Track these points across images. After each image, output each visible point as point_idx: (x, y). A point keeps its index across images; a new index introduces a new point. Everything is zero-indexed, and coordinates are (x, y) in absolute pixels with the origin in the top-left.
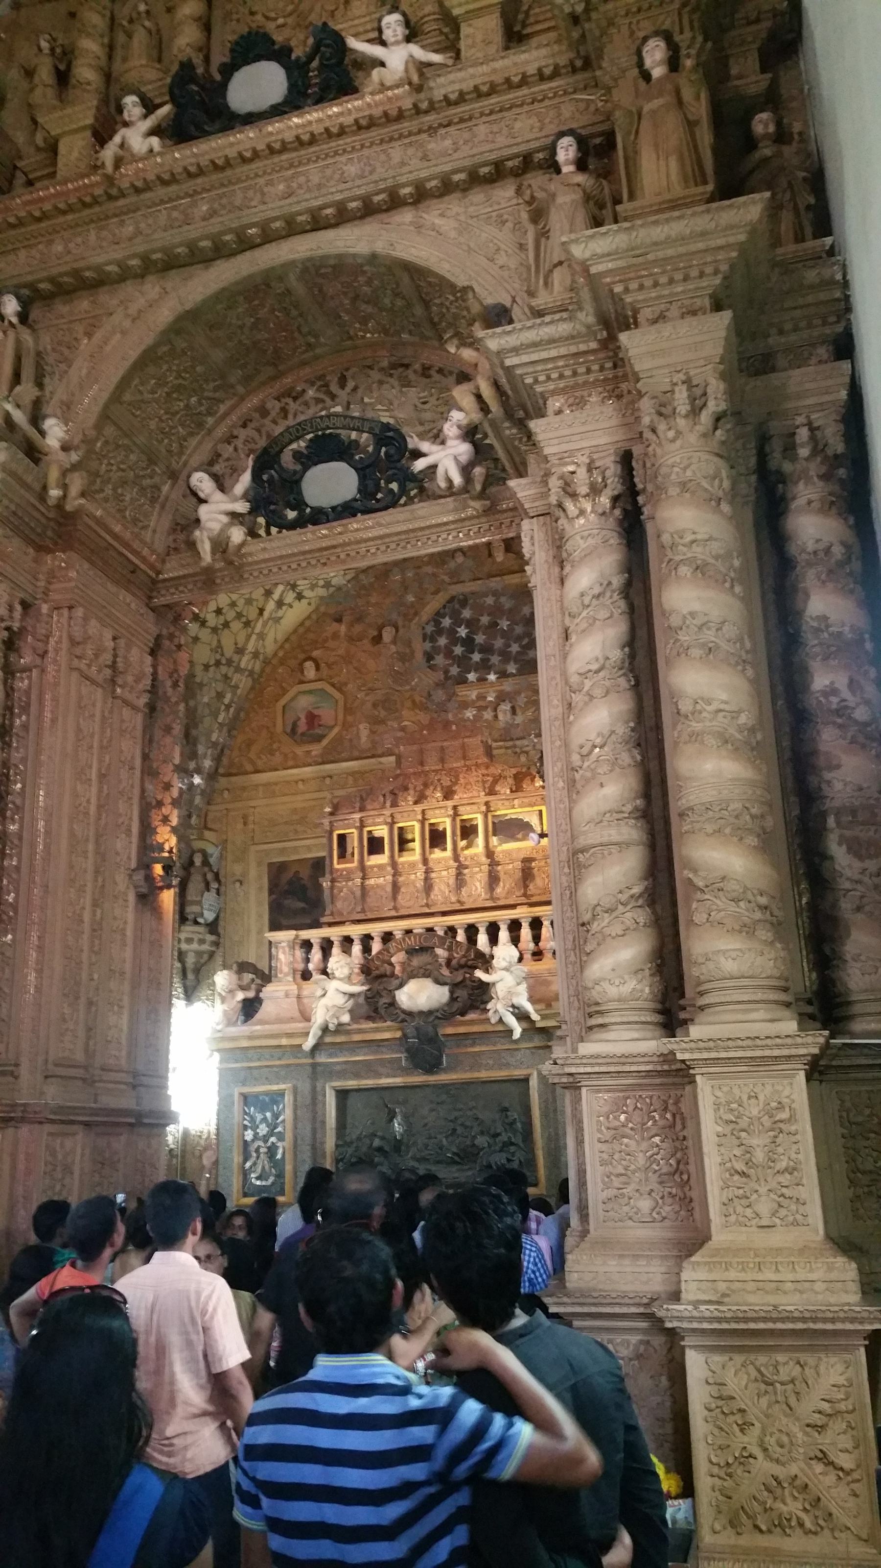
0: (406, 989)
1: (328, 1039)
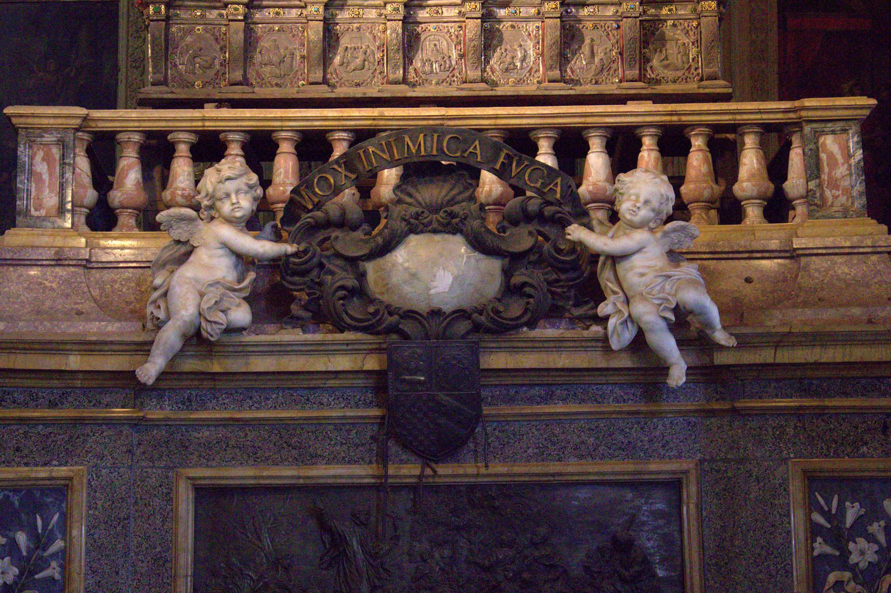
0: (400, 256)
1: (190, 365)
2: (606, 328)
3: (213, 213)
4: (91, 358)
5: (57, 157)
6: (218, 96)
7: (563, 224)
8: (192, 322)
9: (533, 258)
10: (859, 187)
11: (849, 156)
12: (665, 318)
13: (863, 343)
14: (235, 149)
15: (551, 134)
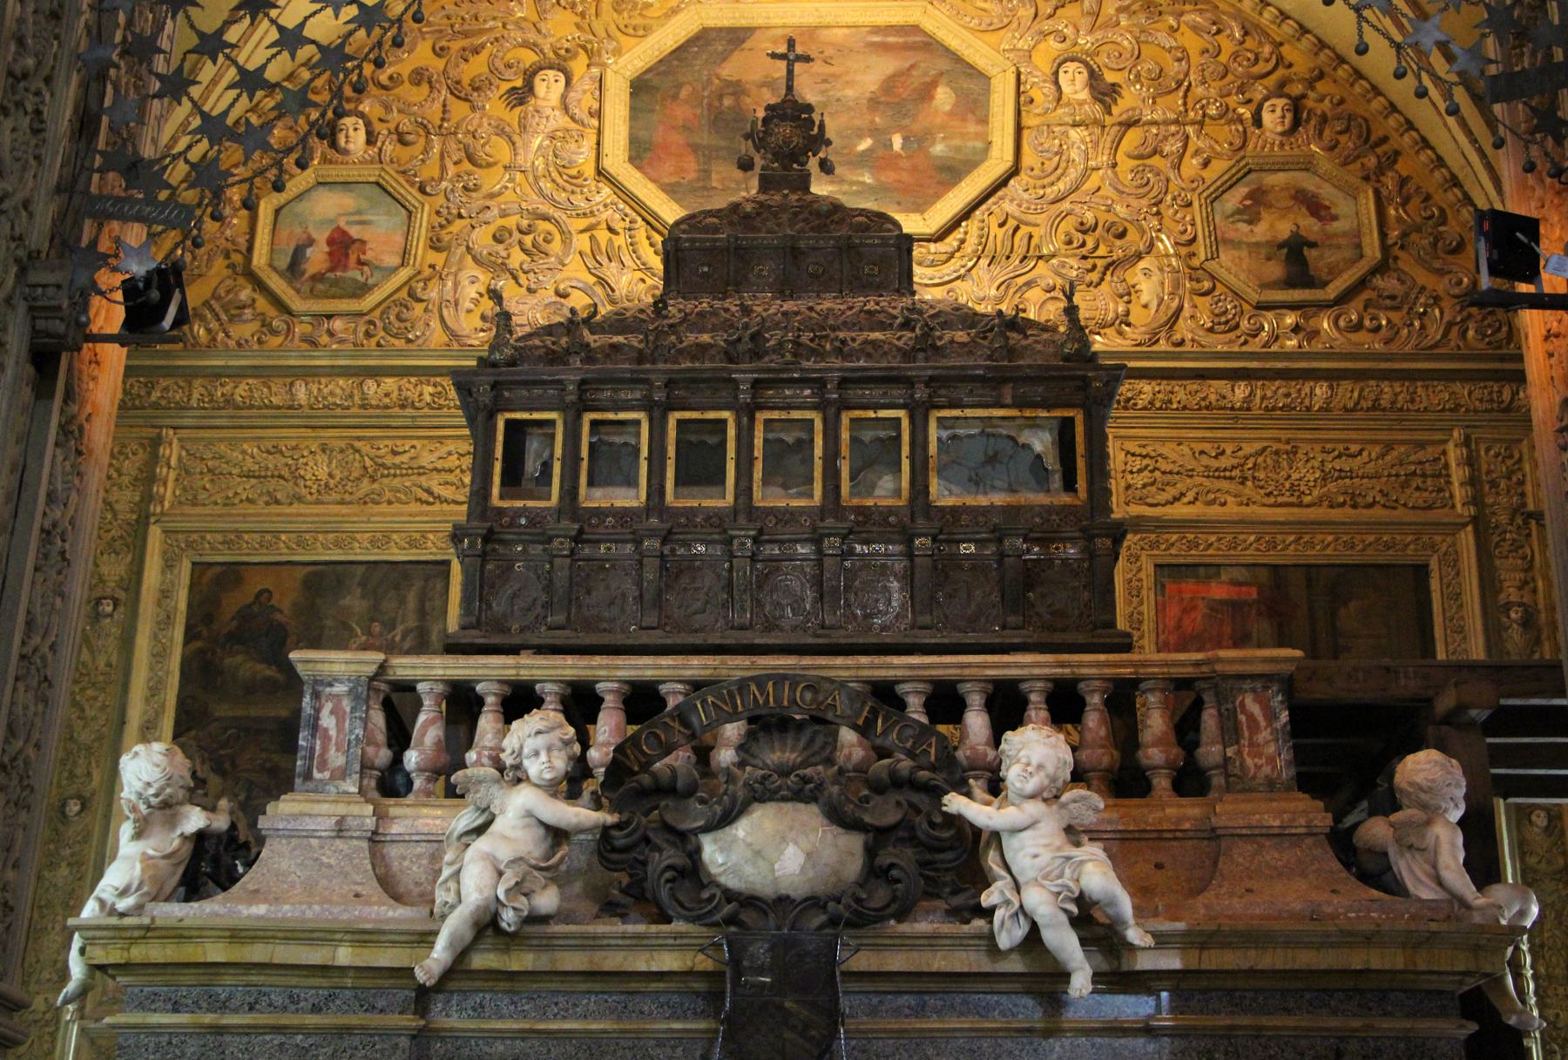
2: (991, 922)
3: (519, 774)
4: (366, 951)
5: (348, 709)
6: (536, 641)
7: (937, 793)
8: (486, 908)
9: (901, 834)
10: (1287, 755)
11: (1271, 716)
12: (1065, 911)
13: (1308, 946)
14: (551, 702)
15: (921, 687)
